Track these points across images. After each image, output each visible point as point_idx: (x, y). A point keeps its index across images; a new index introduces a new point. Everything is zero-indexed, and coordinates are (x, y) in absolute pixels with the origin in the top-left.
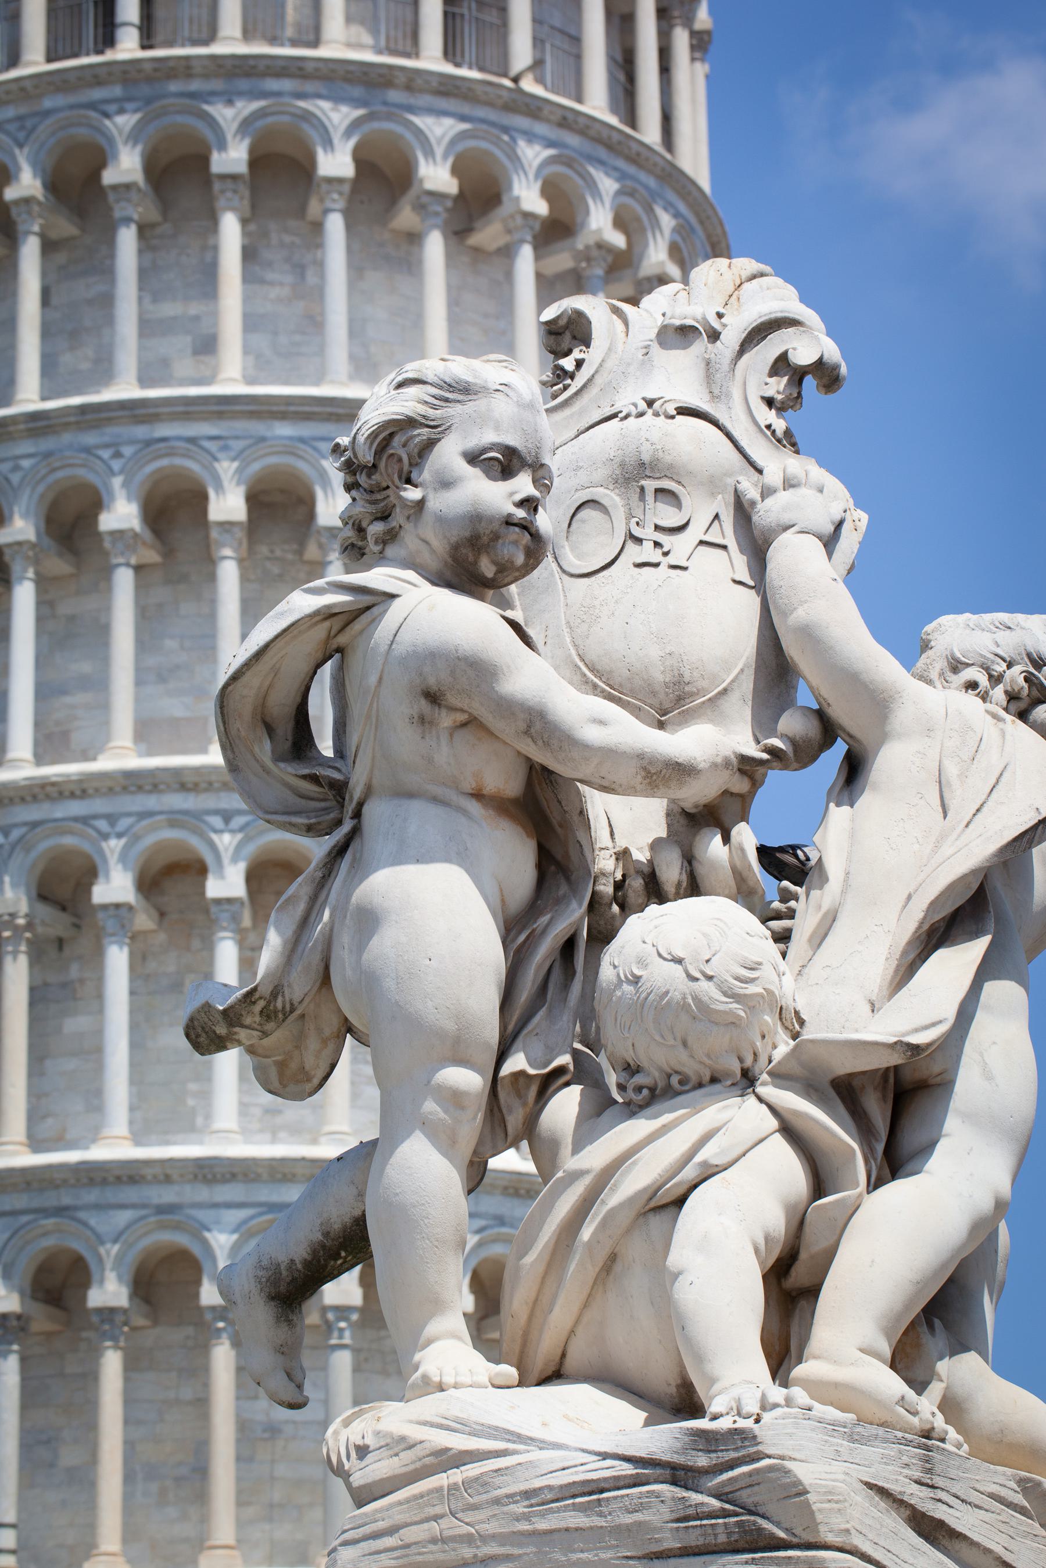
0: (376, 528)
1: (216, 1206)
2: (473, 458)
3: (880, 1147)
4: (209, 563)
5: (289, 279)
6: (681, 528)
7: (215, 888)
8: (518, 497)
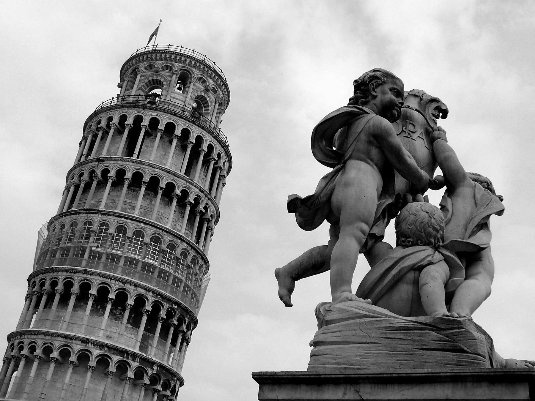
2: (391, 90)
5: (149, 201)
6: (414, 132)
8: (399, 102)
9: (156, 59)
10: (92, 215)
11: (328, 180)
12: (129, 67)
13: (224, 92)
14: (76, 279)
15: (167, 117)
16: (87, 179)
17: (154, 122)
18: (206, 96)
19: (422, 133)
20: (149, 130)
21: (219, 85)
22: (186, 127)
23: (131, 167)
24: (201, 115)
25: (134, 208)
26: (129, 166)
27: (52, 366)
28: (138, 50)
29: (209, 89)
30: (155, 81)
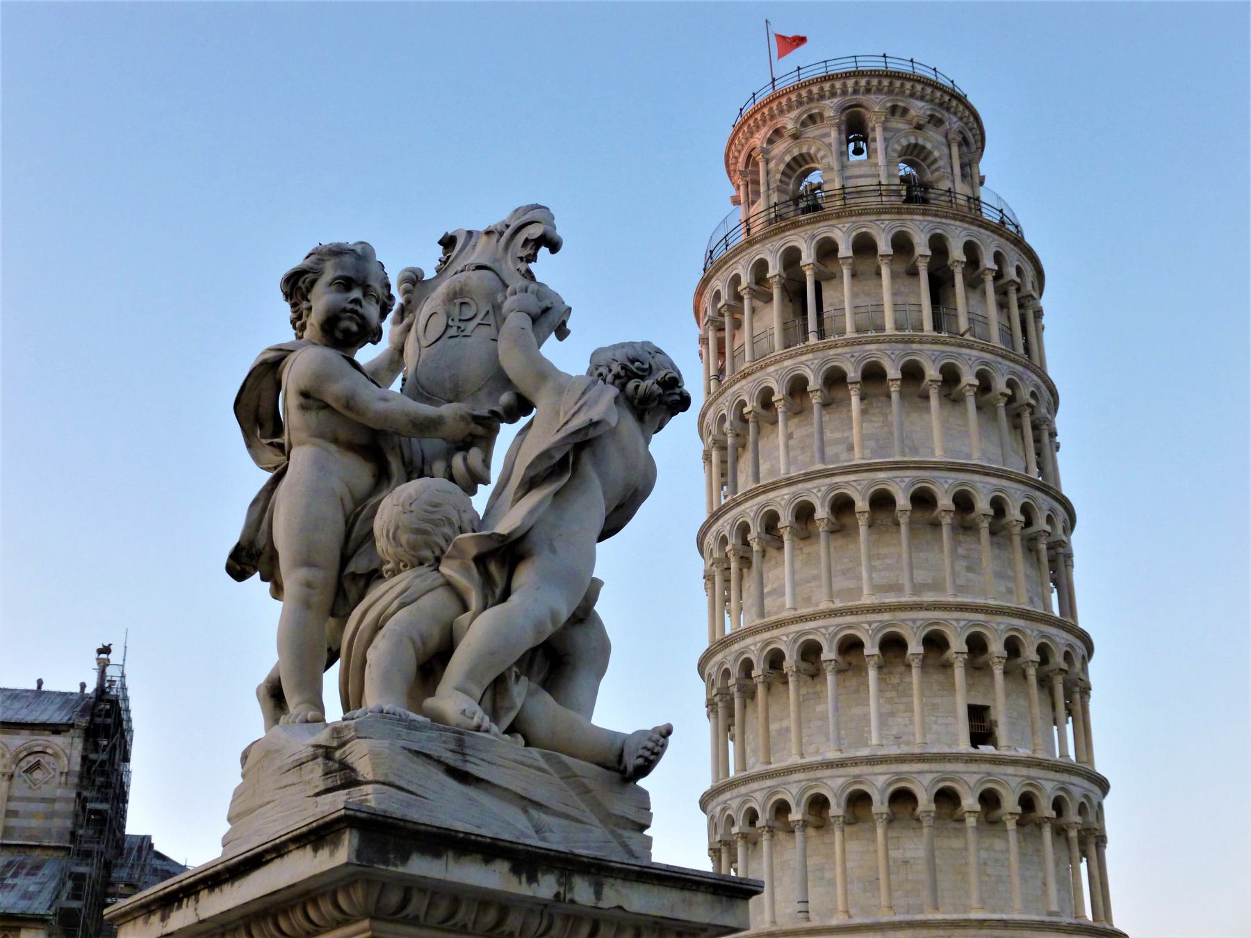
0: (298, 324)
1: (876, 774)
3: (498, 591)
4: (857, 528)
7: (867, 652)
9: (781, 112)
10: (771, 495)
11: (261, 504)
12: (736, 154)
13: (959, 115)
14: (785, 642)
15: (847, 225)
16: (738, 423)
17: (827, 250)
18: (921, 142)
19: (488, 312)
20: (822, 268)
21: (941, 104)
22: (898, 229)
23: (812, 364)
24: (926, 187)
25: (851, 448)
26: (809, 363)
27: (798, 834)
28: (741, 110)
29: (921, 122)
30: (800, 160)
